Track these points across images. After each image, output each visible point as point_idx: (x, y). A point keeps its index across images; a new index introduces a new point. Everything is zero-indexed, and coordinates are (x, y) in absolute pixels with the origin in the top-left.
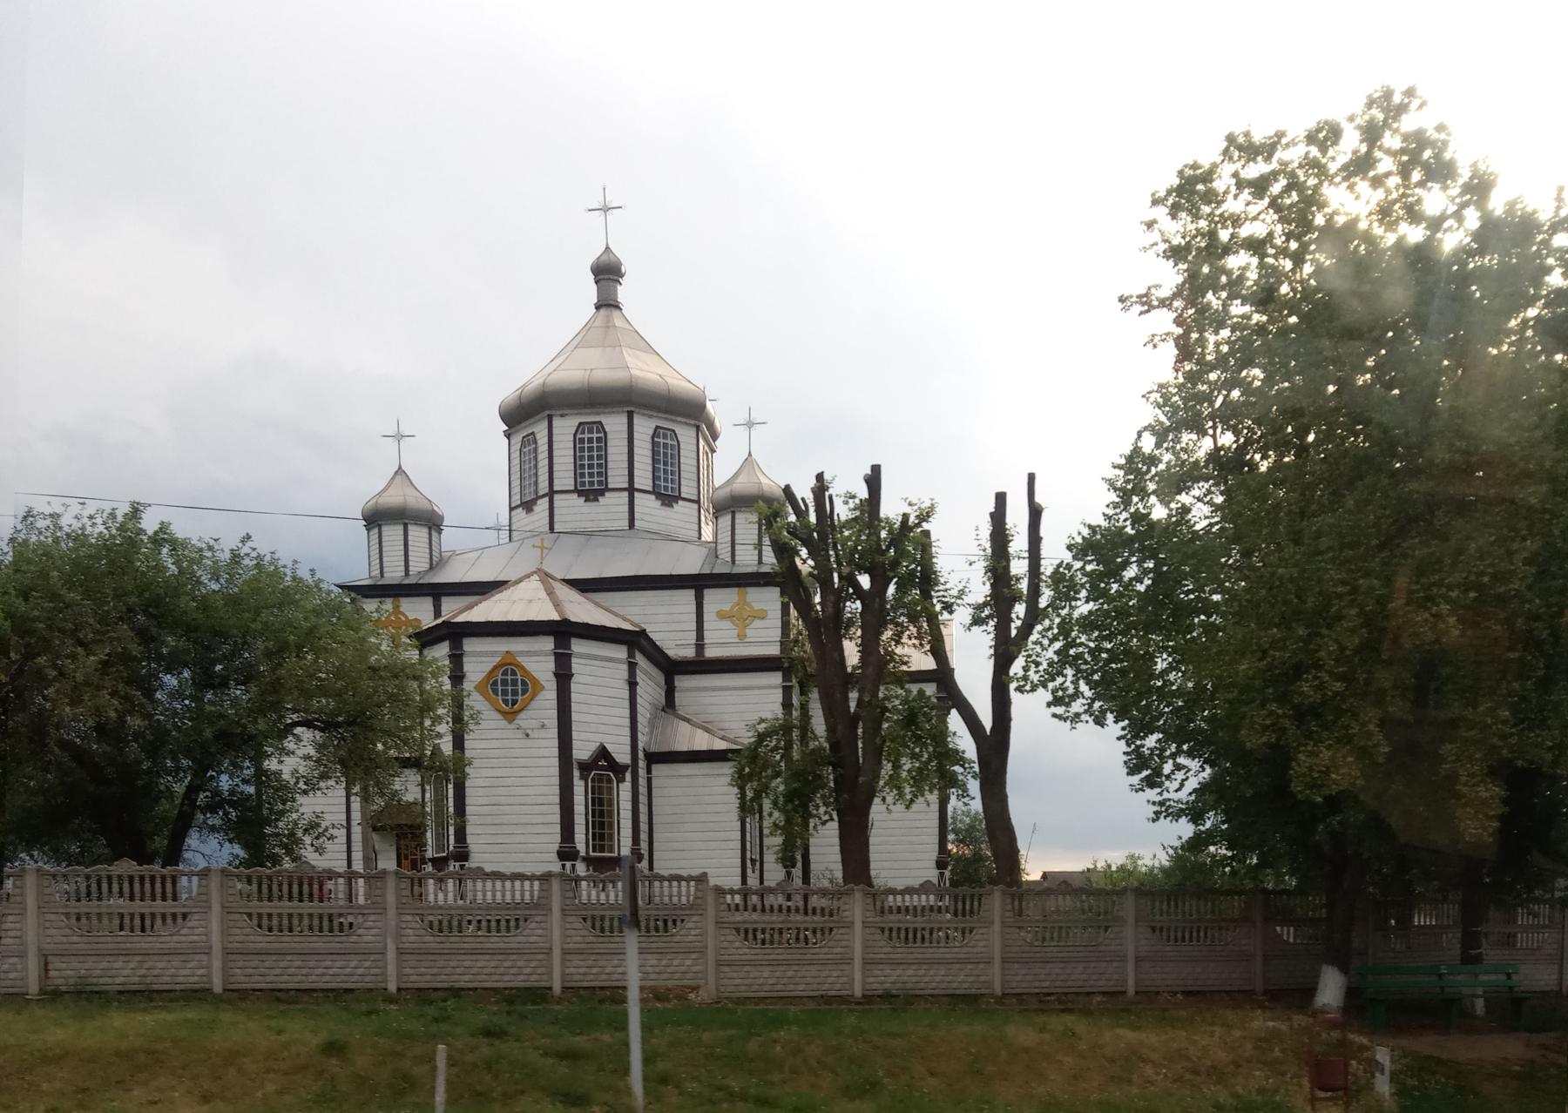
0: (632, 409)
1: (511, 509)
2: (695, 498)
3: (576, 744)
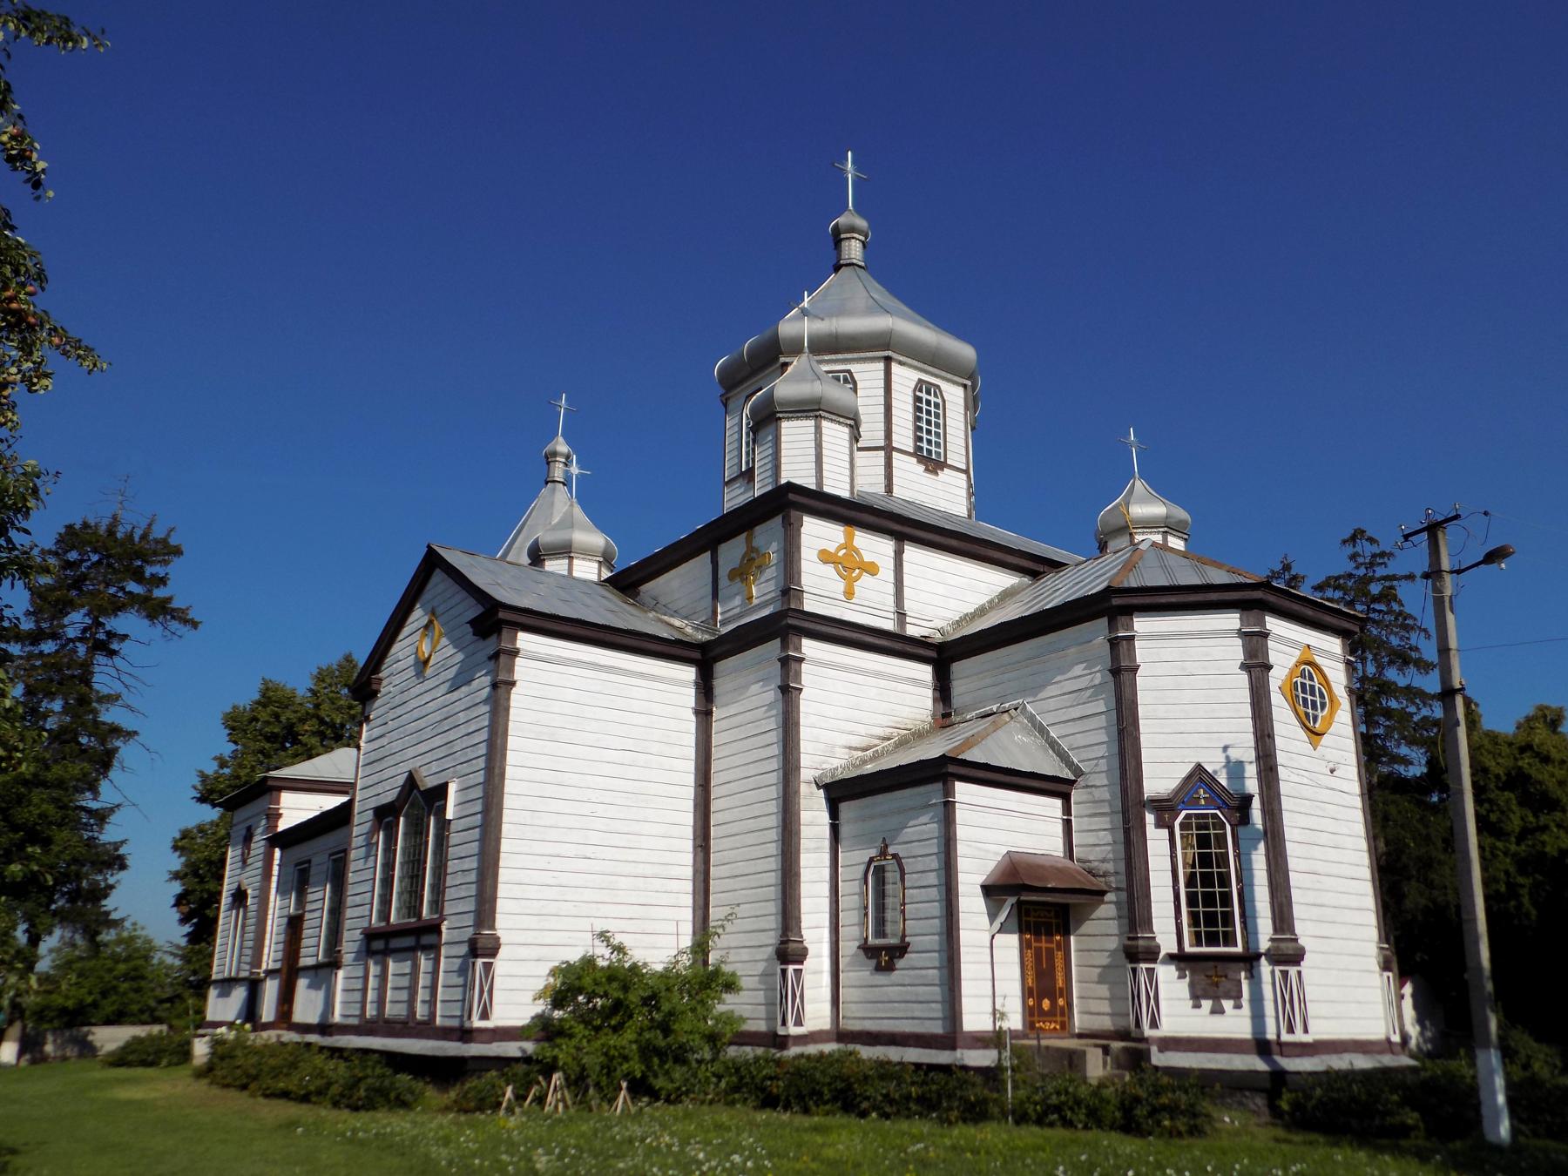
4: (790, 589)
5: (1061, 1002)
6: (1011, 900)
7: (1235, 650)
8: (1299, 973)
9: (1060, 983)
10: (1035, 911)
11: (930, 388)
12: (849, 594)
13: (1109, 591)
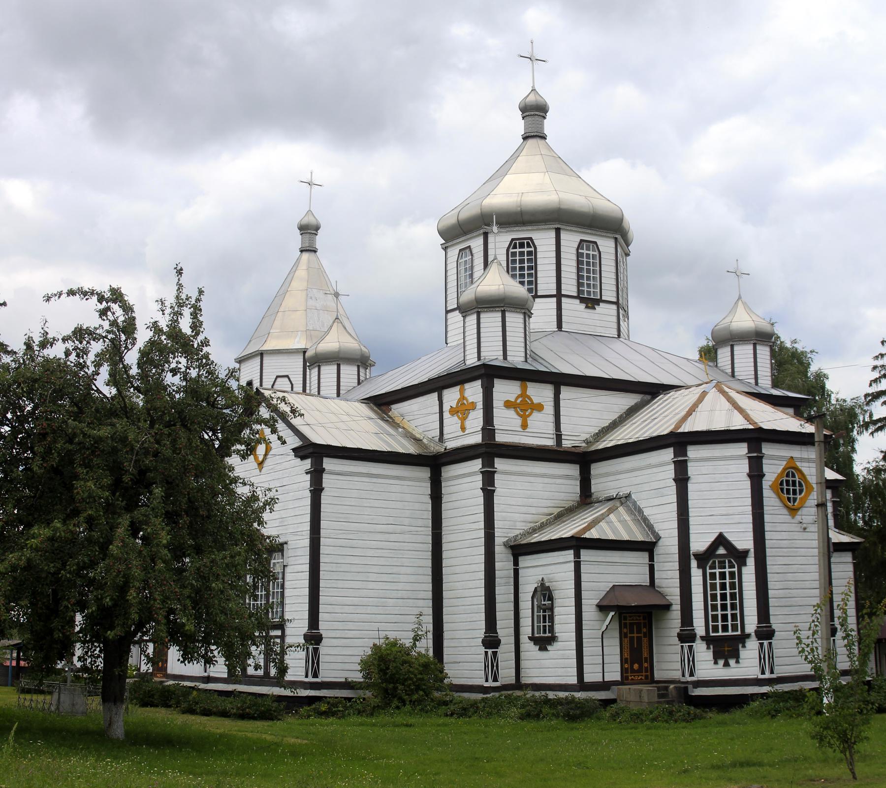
0: (559, 226)
1: (447, 312)
2: (614, 300)
3: (693, 538)
4: (488, 428)
5: (646, 665)
6: (612, 614)
7: (744, 467)
8: (770, 644)
9: (645, 654)
10: (630, 617)
12: (524, 426)
13: (672, 434)
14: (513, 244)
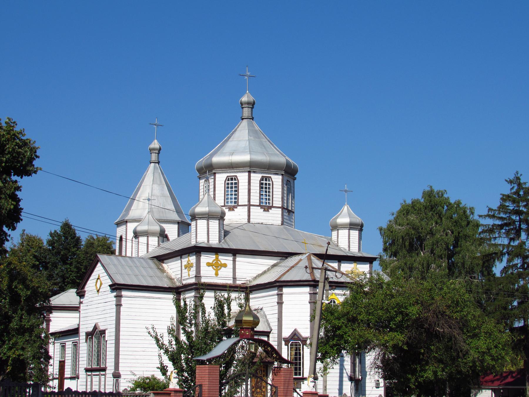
4: (198, 276)
11: (266, 179)
12: (217, 274)
13: (276, 282)
14: (228, 179)
